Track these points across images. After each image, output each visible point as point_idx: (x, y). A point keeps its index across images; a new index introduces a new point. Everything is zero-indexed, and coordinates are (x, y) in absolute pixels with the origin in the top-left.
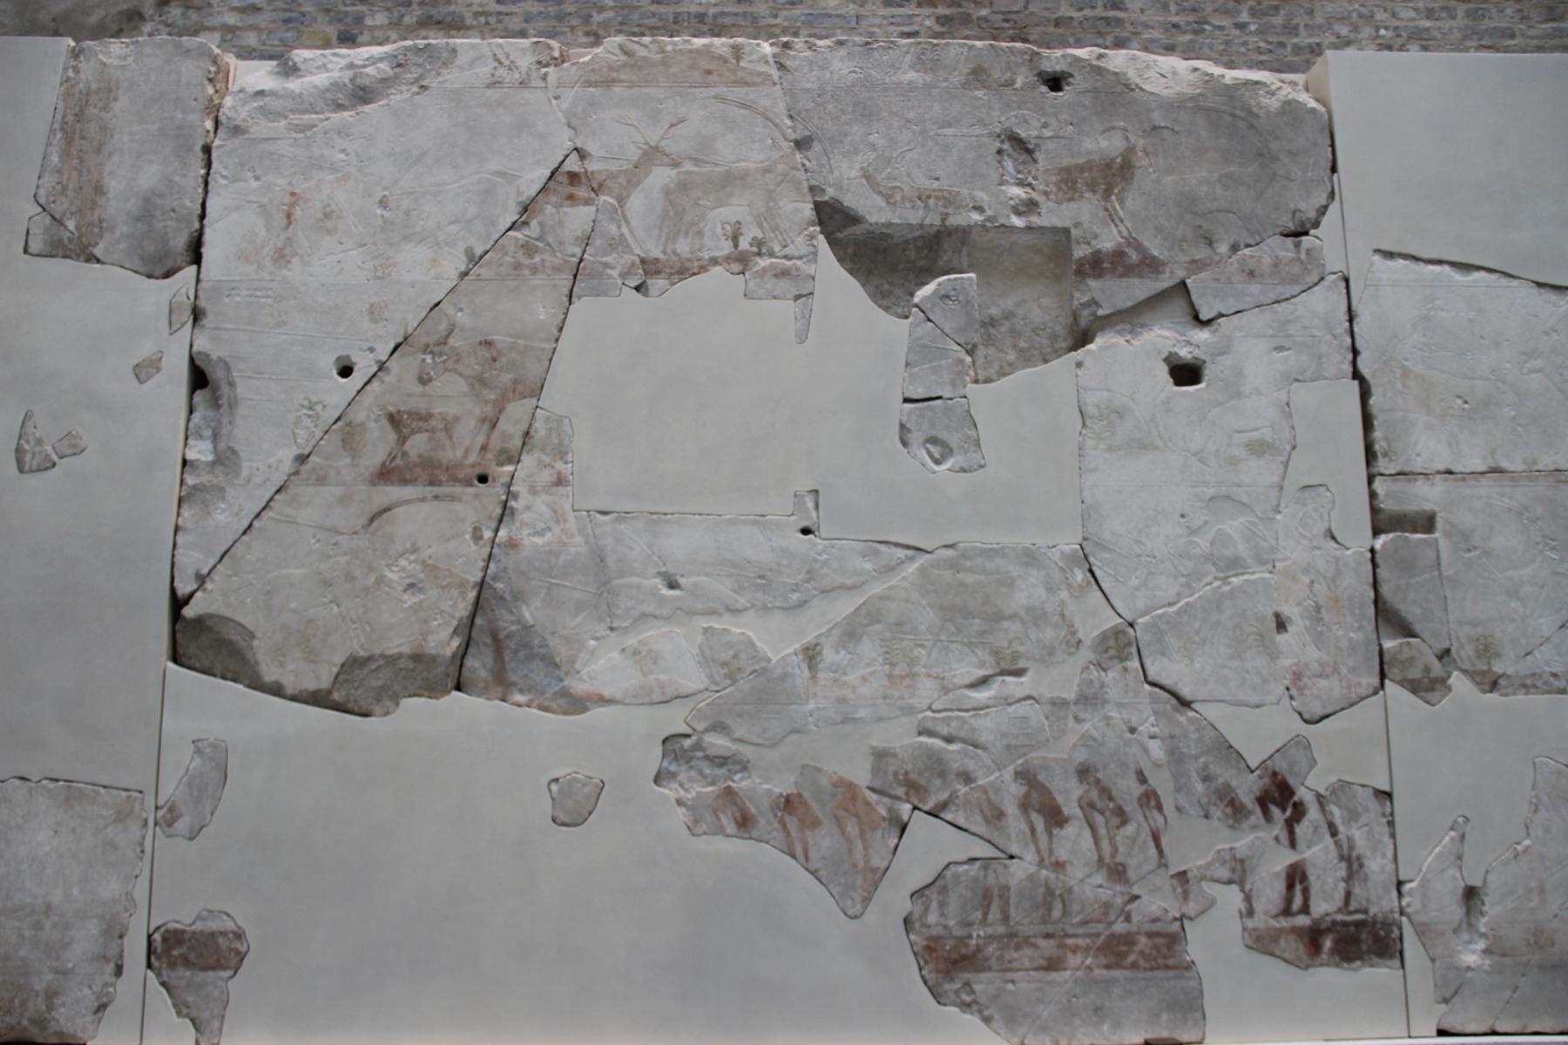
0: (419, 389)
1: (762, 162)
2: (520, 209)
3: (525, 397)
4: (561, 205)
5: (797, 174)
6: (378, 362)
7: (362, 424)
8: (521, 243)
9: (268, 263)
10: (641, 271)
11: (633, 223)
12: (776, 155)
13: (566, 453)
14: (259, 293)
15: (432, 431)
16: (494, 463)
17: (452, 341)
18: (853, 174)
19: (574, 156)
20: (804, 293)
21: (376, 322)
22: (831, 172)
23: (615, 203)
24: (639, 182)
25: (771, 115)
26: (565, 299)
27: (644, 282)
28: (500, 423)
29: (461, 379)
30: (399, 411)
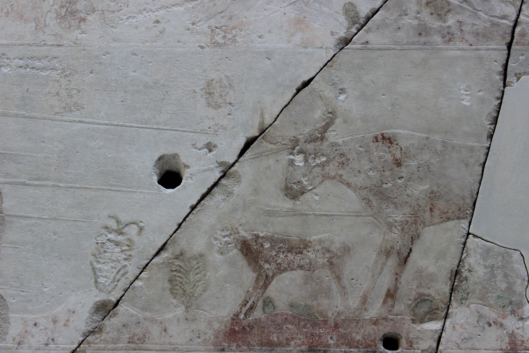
0: (288, 204)
3: (448, 219)
6: (221, 164)
7: (201, 255)
9: (51, 21)
13: (520, 305)
14: (38, 64)
15: (310, 267)
16: (408, 318)
17: (332, 136)
21: (218, 106)
26: (498, 78)
28: (412, 255)
29: (349, 191)
30: (257, 237)
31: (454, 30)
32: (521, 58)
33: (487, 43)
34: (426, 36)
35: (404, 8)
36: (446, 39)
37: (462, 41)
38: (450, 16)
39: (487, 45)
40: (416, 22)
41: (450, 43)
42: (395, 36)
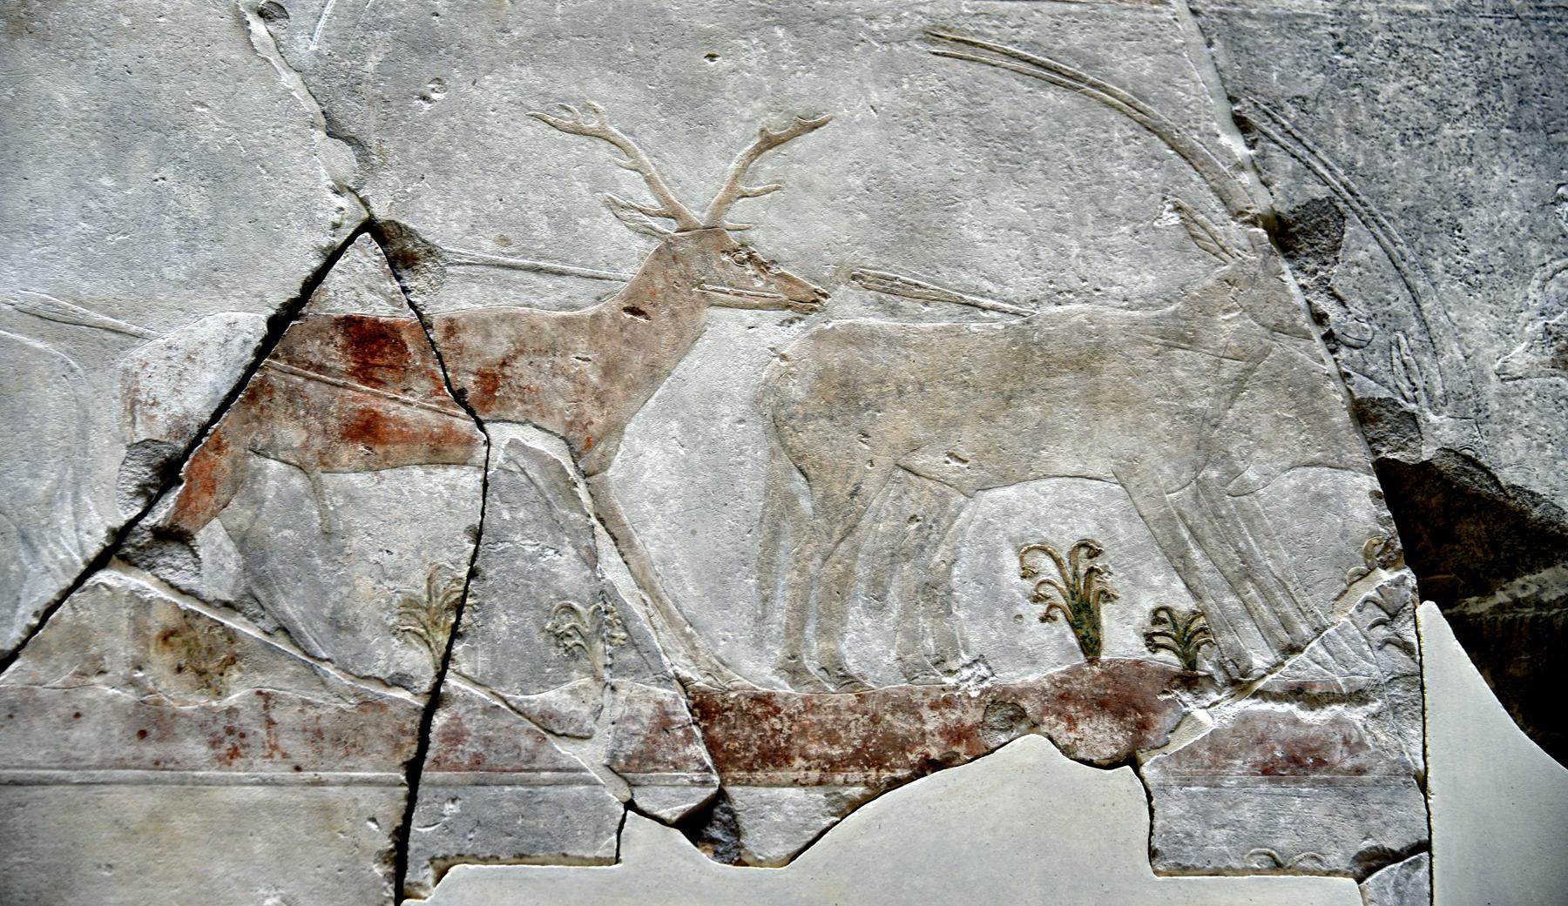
1: (1147, 301)
2: (145, 474)
4: (327, 462)
5: (1284, 346)
8: (161, 619)
10: (700, 750)
11: (651, 540)
12: (1203, 274)
18: (1520, 357)
19: (366, 257)
20: (1393, 843)
22: (1432, 346)
23: (567, 462)
24: (654, 374)
25: (1165, 117)
27: (721, 795)
31: (245, 720)
32: (450, 808)
33: (348, 764)
34: (160, 740)
35: (94, 650)
36: (223, 751)
37: (271, 756)
38: (236, 675)
39: (347, 769)
40: (129, 696)
41: (236, 762)
42: (66, 740)
